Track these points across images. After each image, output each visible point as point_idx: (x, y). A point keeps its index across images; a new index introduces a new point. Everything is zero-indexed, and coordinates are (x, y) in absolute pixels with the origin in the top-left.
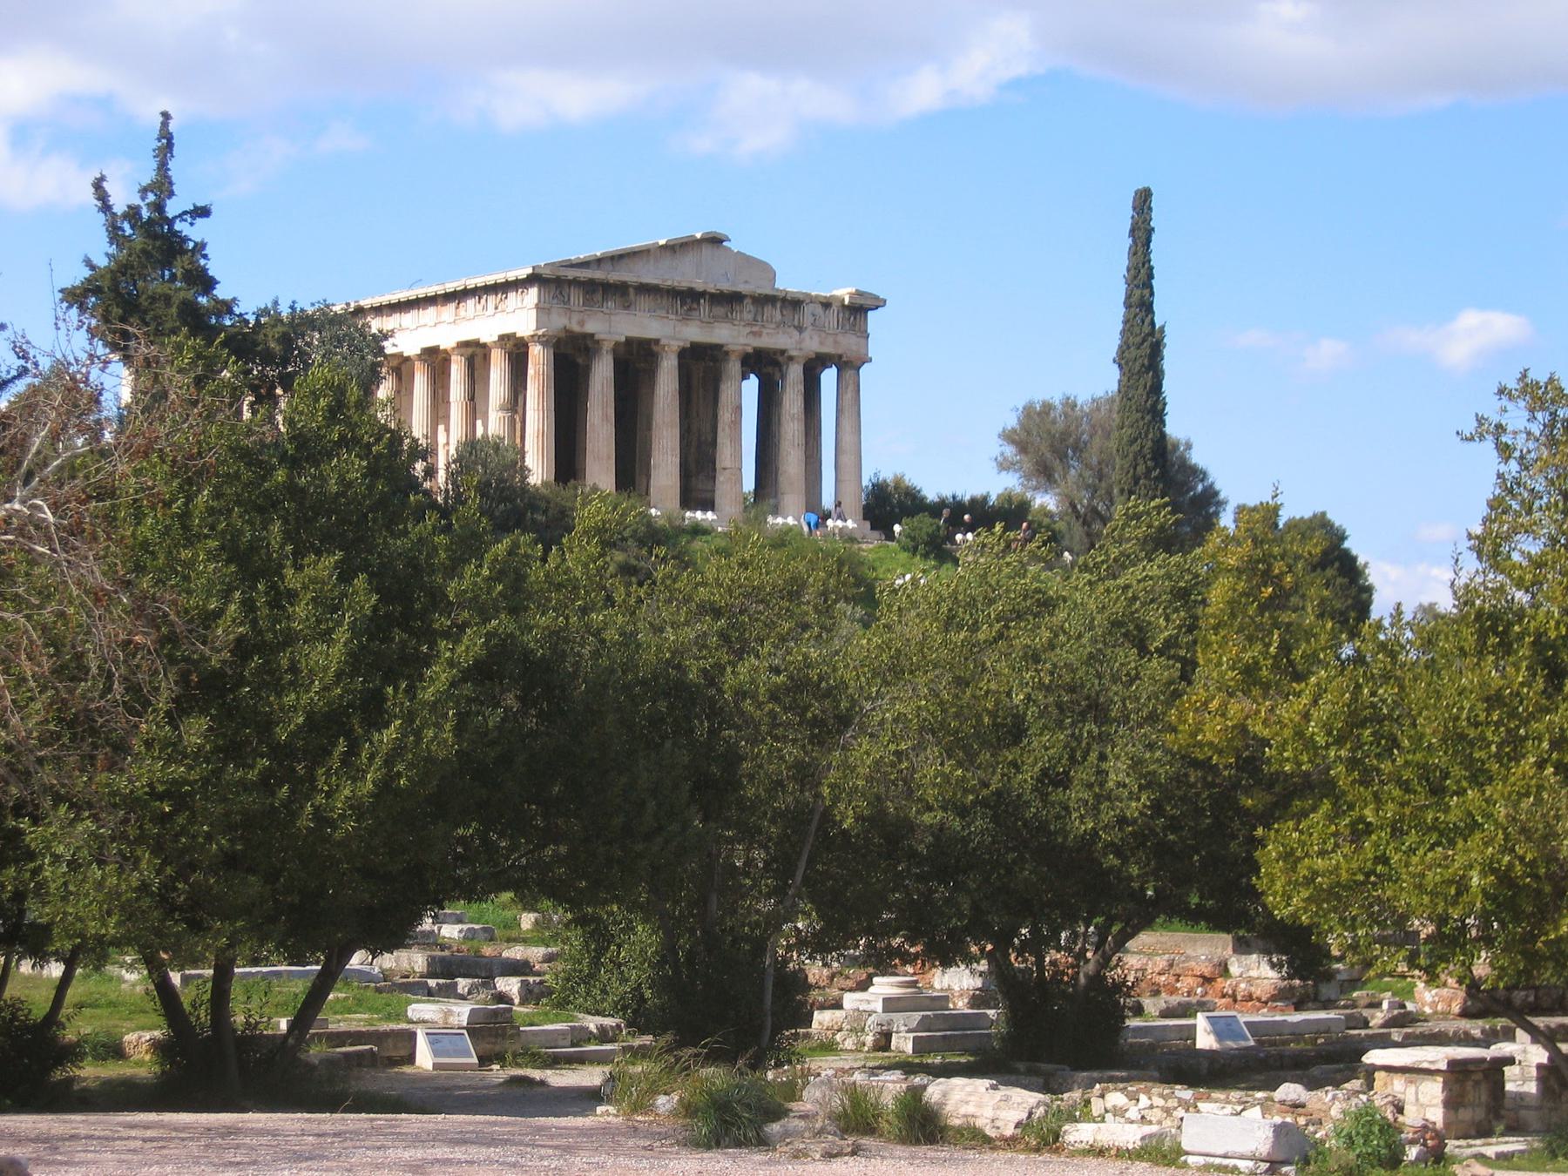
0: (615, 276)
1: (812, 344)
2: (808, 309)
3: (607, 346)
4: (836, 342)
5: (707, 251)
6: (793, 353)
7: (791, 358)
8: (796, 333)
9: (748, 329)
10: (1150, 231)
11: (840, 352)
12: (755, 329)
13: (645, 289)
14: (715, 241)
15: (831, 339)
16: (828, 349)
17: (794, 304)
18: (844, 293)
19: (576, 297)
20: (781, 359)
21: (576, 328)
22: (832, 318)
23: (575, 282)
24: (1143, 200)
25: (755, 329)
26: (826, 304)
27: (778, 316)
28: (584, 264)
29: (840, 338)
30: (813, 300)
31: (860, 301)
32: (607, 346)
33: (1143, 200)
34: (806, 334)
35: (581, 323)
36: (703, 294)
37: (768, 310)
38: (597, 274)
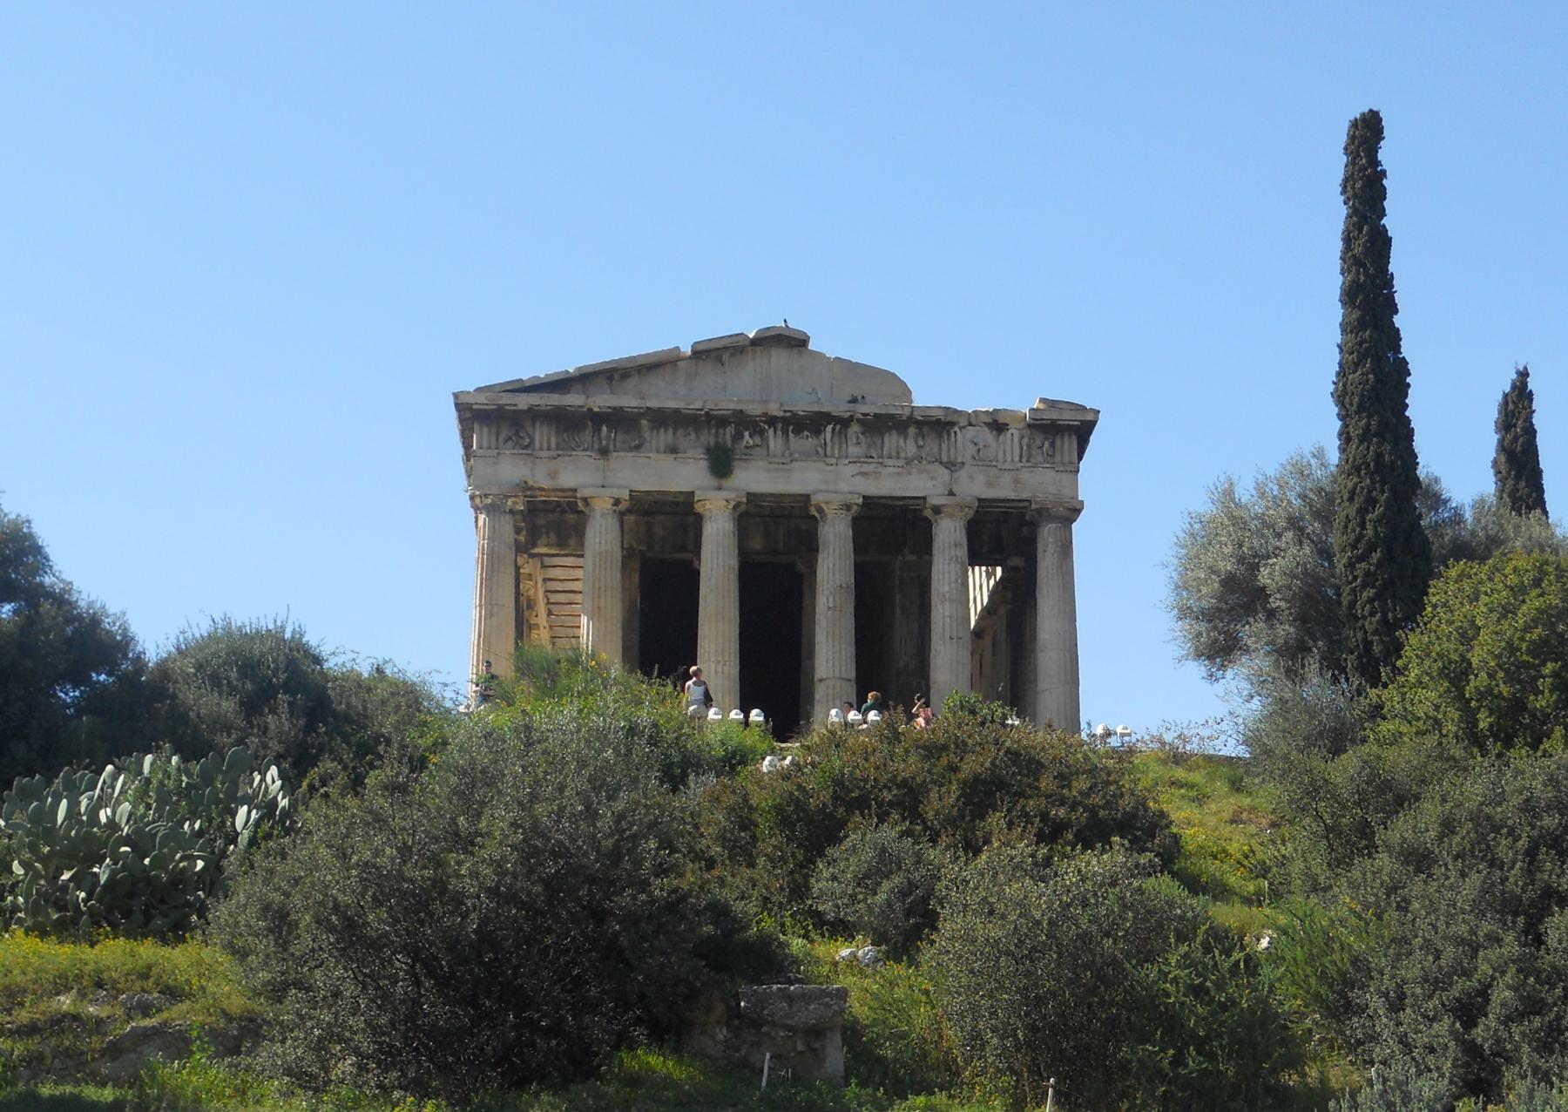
0: (601, 400)
1: (975, 486)
2: (964, 437)
3: (602, 505)
4: (1017, 481)
5: (779, 358)
6: (935, 501)
7: (937, 510)
8: (943, 473)
9: (854, 468)
11: (1024, 496)
12: (866, 468)
13: (663, 419)
14: (793, 342)
15: (1007, 478)
17: (940, 425)
18: (1022, 401)
20: (928, 513)
21: (545, 483)
22: (1012, 441)
23: (534, 414)
24: (1367, 134)
25: (866, 468)
26: (996, 423)
27: (910, 448)
28: (560, 384)
29: (1025, 475)
30: (972, 419)
31: (1054, 415)
32: (602, 505)
33: (1367, 134)
34: (963, 474)
35: (553, 475)
36: (772, 421)
37: (891, 440)
38: (573, 400)
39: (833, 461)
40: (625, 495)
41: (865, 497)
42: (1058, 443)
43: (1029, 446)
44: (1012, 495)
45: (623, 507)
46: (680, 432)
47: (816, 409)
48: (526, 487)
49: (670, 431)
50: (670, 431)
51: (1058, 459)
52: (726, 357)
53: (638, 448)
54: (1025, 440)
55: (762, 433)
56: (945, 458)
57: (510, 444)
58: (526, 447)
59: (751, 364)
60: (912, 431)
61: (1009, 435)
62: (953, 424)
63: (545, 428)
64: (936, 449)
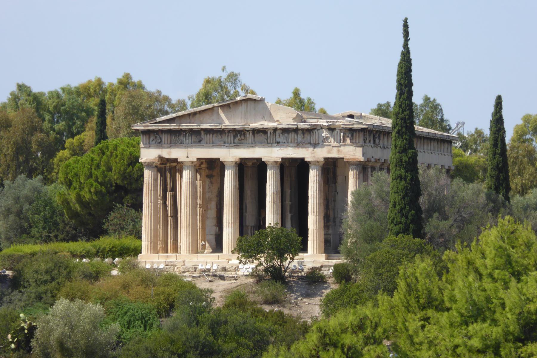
0: (185, 126)
4: (339, 151)
10: (410, 84)
11: (341, 156)
13: (208, 131)
16: (334, 154)
19: (165, 138)
21: (167, 156)
27: (300, 138)
29: (342, 148)
31: (351, 127)
35: (169, 153)
39: (270, 145)
40: (195, 160)
41: (282, 159)
42: (354, 135)
43: (344, 136)
44: (336, 156)
45: (194, 164)
46: (215, 135)
47: (262, 127)
48: (161, 158)
49: (211, 135)
50: (211, 135)
51: (354, 141)
52: (231, 106)
53: (200, 141)
54: (342, 134)
55: (244, 134)
56: (312, 142)
57: (154, 142)
58: (159, 143)
59: (240, 107)
60: (300, 132)
61: (336, 132)
62: (315, 129)
63: (166, 135)
64: (309, 138)
